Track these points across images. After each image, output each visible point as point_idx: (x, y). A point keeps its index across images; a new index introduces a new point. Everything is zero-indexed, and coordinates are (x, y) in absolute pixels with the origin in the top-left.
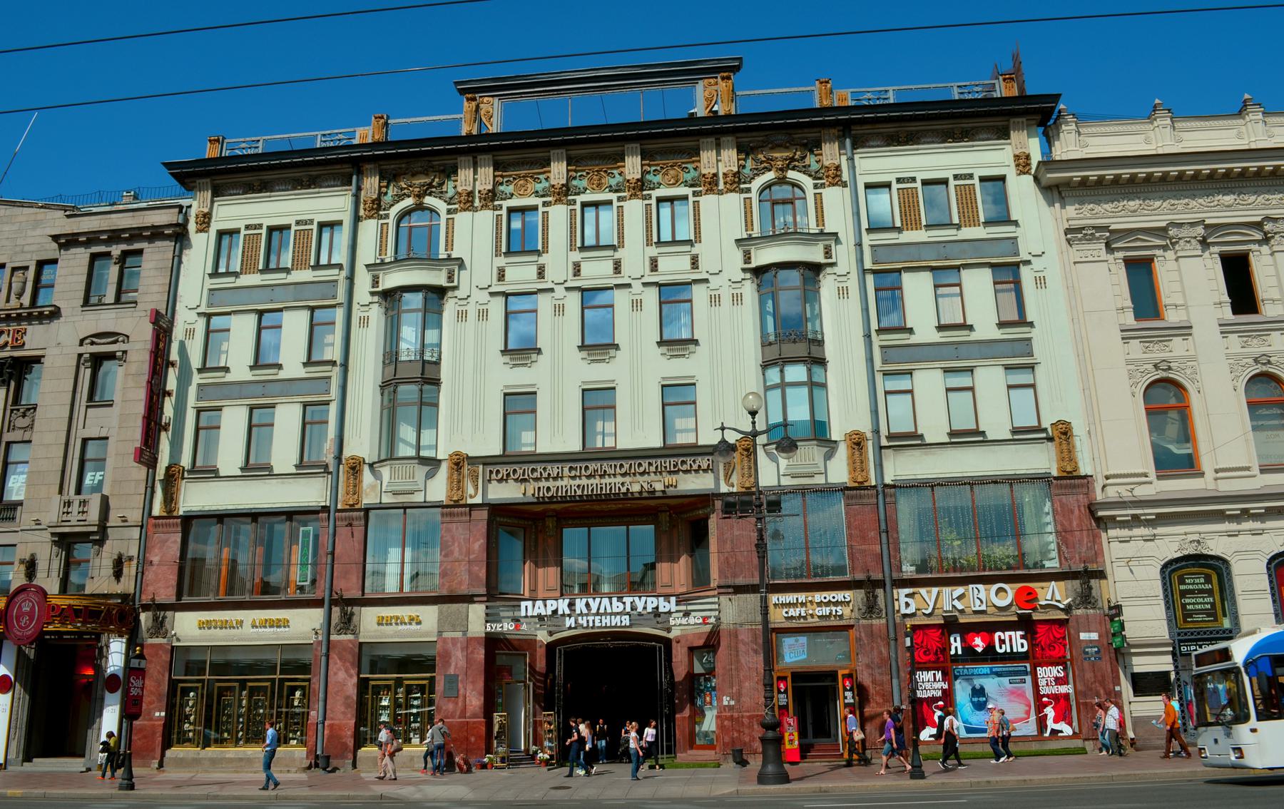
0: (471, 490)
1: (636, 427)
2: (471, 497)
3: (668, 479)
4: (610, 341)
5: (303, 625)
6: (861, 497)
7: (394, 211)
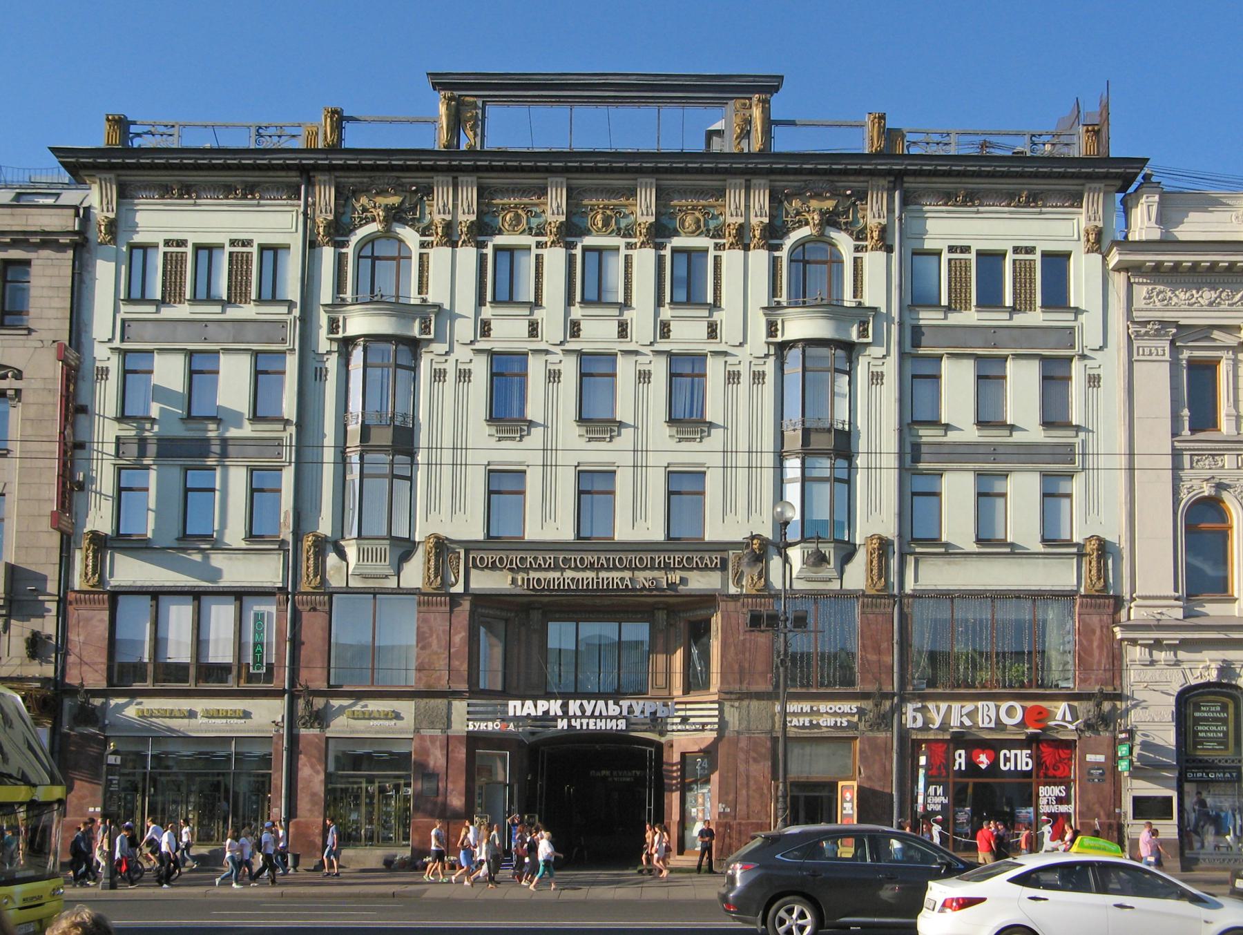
1: (639, 519)
2: (453, 585)
3: (675, 577)
4: (609, 417)
5: (267, 714)
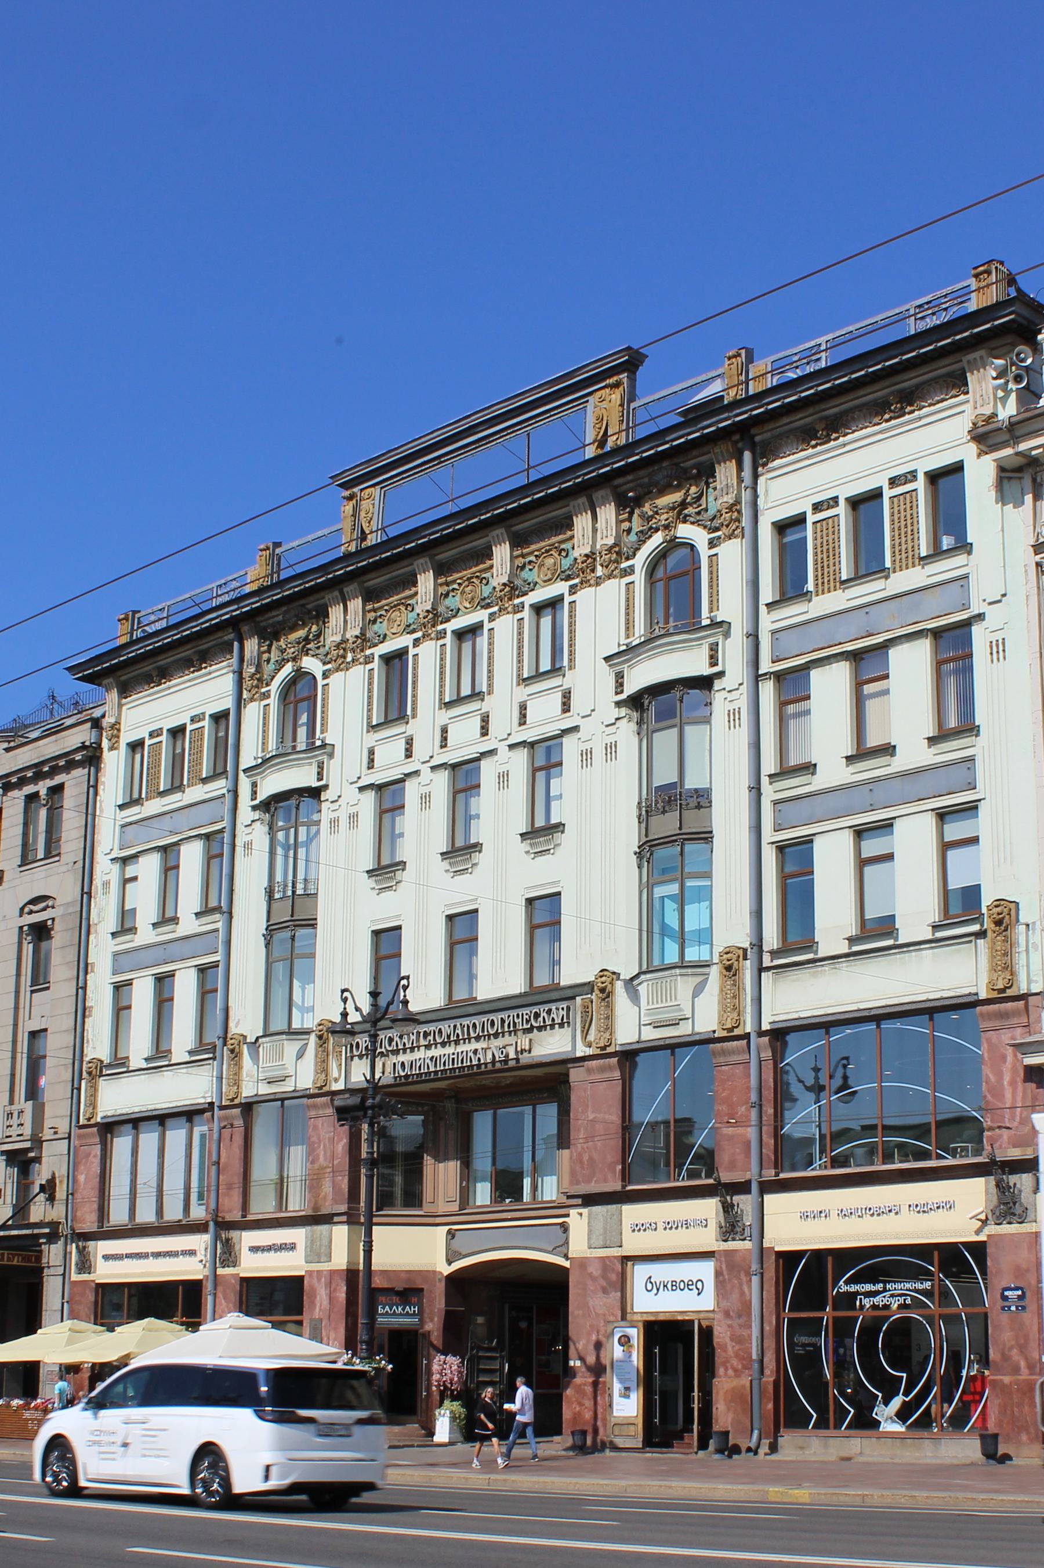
0: (335, 1074)
3: (524, 1042)
6: (724, 1053)
7: (275, 687)
